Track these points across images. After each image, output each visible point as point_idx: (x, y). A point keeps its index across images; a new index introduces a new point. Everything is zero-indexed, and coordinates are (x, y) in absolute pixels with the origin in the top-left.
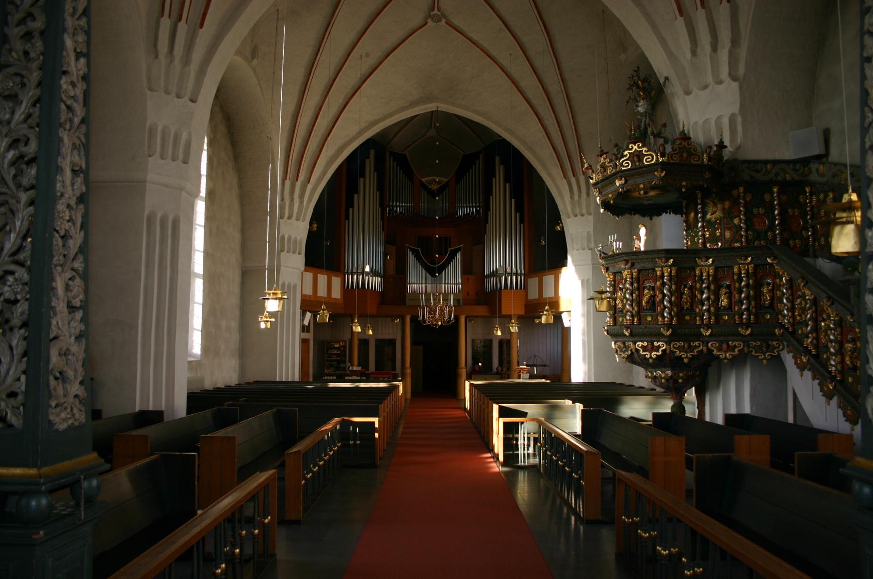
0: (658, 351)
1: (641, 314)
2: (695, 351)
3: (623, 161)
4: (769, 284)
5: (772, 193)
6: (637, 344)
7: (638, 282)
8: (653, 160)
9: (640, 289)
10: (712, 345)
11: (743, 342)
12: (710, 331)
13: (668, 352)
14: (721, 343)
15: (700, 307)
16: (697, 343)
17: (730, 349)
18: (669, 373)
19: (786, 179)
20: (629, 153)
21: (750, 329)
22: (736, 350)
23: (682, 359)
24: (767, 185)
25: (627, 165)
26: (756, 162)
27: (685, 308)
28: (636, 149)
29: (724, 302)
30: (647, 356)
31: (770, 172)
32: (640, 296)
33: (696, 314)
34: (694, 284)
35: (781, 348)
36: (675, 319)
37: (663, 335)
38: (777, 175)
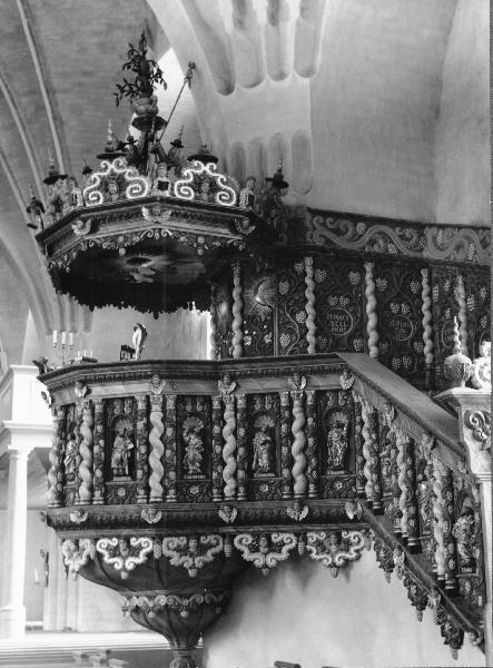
0: (137, 556)
1: (107, 483)
2: (209, 553)
3: (89, 191)
4: (340, 426)
5: (363, 272)
6: (99, 542)
7: (104, 423)
8: (143, 191)
9: (109, 436)
10: (240, 542)
11: (297, 535)
12: (235, 513)
13: (156, 556)
14: (257, 536)
15: (219, 468)
16: (211, 539)
17: (274, 548)
18: (162, 600)
19: (387, 250)
20: (99, 176)
21: (306, 510)
22: (285, 549)
23: (186, 570)
24: (356, 260)
25: (95, 198)
26: (337, 216)
27: (191, 472)
28: (112, 171)
29: (264, 461)
30: (116, 566)
31: (361, 236)
32: (109, 449)
33: (211, 483)
34: (209, 427)
35: (362, 543)
36: (172, 491)
37: (144, 524)
38: (372, 242)
